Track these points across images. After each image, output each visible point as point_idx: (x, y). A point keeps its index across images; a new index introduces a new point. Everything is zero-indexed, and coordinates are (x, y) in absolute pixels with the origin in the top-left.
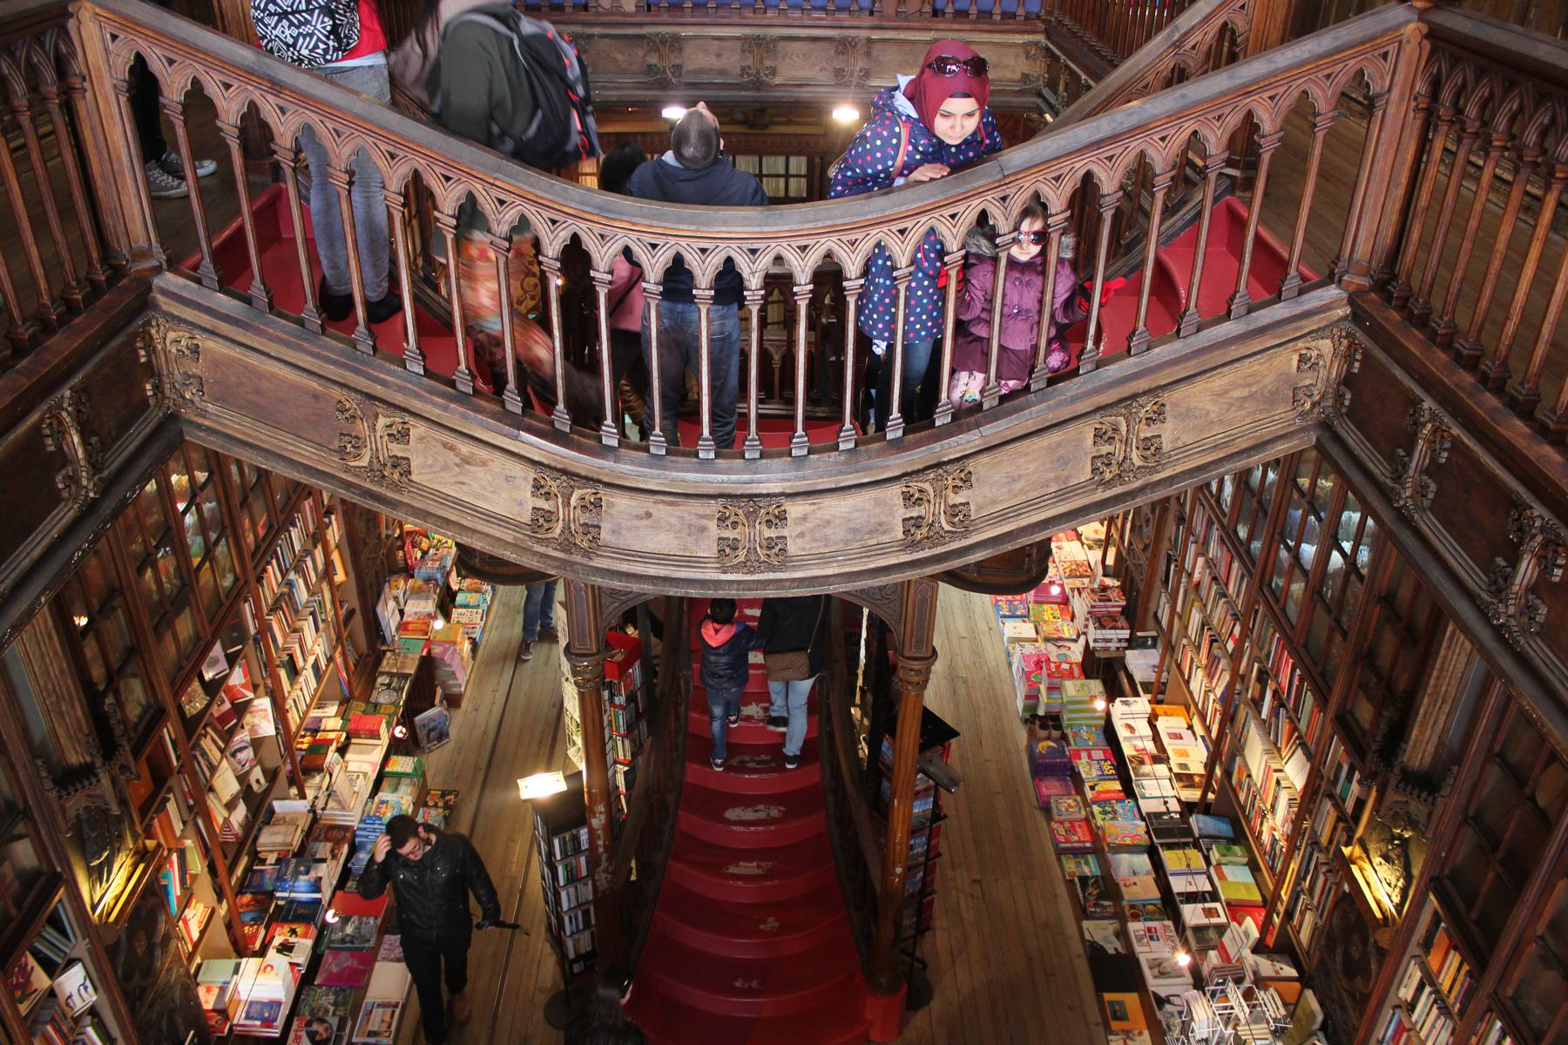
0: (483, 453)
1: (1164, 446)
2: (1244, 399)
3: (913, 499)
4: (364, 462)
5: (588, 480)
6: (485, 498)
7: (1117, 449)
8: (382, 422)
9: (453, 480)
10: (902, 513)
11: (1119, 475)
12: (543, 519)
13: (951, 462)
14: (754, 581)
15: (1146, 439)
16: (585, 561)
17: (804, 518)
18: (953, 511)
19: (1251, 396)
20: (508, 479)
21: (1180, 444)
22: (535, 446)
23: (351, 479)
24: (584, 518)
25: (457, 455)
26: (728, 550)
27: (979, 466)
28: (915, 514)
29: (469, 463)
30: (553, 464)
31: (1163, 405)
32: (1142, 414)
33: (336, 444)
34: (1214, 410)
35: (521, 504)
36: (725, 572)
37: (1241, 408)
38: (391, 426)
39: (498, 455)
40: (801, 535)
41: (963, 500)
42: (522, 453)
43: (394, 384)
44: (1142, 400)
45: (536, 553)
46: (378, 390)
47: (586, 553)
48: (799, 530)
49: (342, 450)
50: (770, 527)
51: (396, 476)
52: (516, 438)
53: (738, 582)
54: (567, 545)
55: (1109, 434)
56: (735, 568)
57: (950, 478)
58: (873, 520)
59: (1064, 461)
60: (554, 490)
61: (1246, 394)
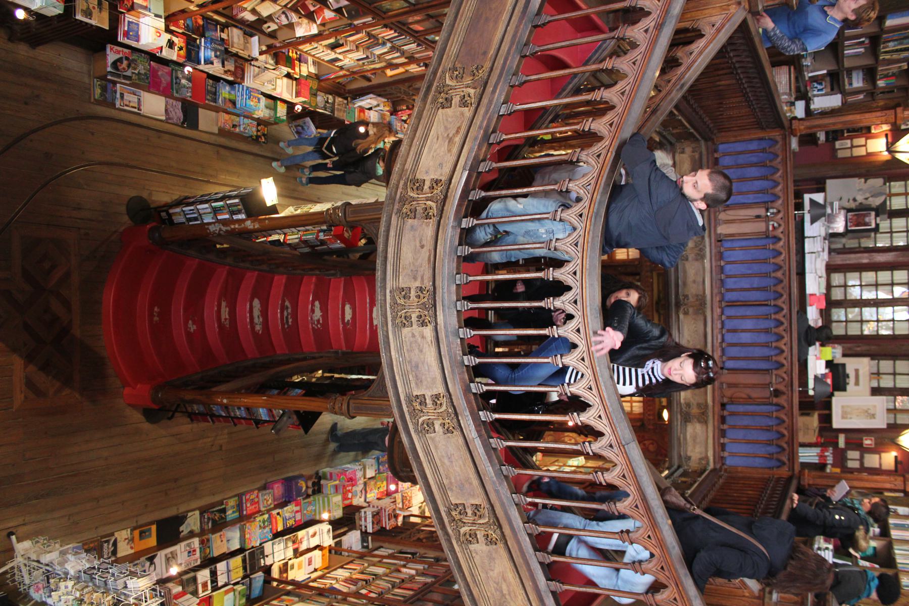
0: (455, 150)
1: (473, 545)
2: (501, 592)
3: (436, 400)
4: (448, 82)
5: (442, 211)
6: (429, 152)
7: (469, 518)
8: (472, 91)
9: (440, 133)
10: (428, 394)
11: (454, 520)
12: (418, 185)
13: (458, 421)
14: (386, 309)
15: (476, 535)
16: (395, 211)
17: (423, 337)
18: (430, 424)
19: (503, 595)
20: (441, 165)
21: (474, 555)
22: (461, 179)
23: (438, 74)
24: (420, 210)
25: (454, 135)
26: (403, 293)
27: (457, 438)
28: (428, 401)
29: (449, 142)
30: (450, 190)
31: (496, 544)
32: (490, 532)
33: (458, 65)
34: (494, 574)
35: (427, 172)
36: (391, 292)
37: (496, 590)
38: (469, 96)
39: (455, 158)
40: (413, 336)
41: (436, 430)
42: (456, 173)
43: (493, 99)
44: (498, 531)
45: (399, 182)
46: (490, 89)
47: (399, 211)
48: (416, 334)
49: (455, 69)
50: (417, 317)
51: (441, 100)
52: (464, 169)
53: (385, 300)
54: (404, 200)
55: (478, 513)
56: (393, 298)
57: (449, 421)
58: (423, 377)
59: (461, 487)
60: (435, 192)
61: (504, 592)
